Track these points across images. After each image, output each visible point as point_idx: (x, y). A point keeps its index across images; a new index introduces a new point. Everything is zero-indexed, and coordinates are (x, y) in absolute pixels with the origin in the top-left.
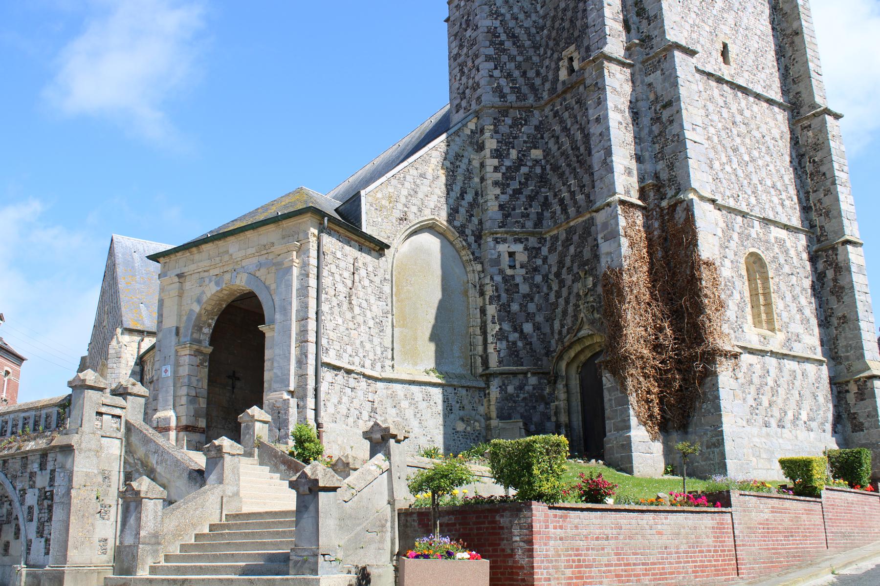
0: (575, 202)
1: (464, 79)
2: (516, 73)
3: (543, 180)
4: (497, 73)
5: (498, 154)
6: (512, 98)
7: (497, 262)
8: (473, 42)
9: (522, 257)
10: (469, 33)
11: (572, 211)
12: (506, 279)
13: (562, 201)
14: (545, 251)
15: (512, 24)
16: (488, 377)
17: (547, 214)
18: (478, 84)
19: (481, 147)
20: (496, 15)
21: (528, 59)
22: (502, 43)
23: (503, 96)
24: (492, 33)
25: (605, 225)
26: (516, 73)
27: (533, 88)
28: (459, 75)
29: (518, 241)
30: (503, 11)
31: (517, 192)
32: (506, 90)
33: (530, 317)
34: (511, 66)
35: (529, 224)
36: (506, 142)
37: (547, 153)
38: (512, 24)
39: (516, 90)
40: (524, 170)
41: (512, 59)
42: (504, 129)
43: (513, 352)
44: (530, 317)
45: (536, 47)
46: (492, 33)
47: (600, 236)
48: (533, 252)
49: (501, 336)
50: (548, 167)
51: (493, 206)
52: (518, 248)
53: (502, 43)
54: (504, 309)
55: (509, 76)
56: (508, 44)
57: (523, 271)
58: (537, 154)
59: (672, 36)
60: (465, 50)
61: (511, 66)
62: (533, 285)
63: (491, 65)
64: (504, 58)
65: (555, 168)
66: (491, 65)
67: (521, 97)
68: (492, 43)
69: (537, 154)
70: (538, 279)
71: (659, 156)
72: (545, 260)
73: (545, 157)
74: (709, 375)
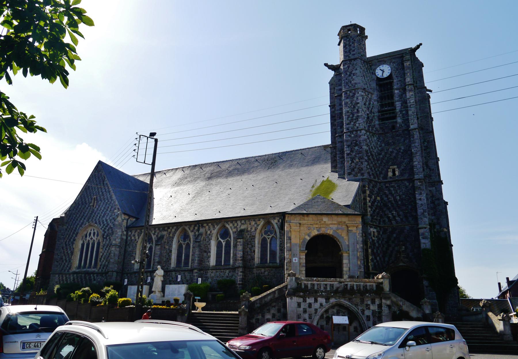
0: (395, 220)
1: (353, 164)
2: (373, 168)
4: (368, 167)
6: (372, 177)
10: (356, 148)
11: (393, 222)
13: (388, 218)
14: (381, 233)
15: (371, 150)
17: (381, 220)
18: (362, 169)
20: (367, 145)
21: (376, 164)
22: (369, 156)
23: (370, 176)
25: (423, 234)
26: (373, 168)
27: (377, 174)
28: (350, 162)
29: (375, 228)
30: (369, 144)
31: (374, 211)
32: (371, 174)
34: (371, 165)
35: (377, 223)
36: (371, 192)
37: (382, 199)
38: (371, 150)
40: (376, 203)
41: (372, 163)
42: (371, 188)
46: (366, 151)
47: (421, 237)
50: (382, 204)
53: (369, 156)
55: (371, 169)
56: (371, 157)
57: (376, 239)
60: (354, 154)
61: (371, 165)
62: (379, 244)
63: (366, 163)
64: (370, 162)
66: (366, 163)
67: (375, 178)
68: (367, 155)
70: (380, 242)
72: (381, 235)
73: (381, 200)
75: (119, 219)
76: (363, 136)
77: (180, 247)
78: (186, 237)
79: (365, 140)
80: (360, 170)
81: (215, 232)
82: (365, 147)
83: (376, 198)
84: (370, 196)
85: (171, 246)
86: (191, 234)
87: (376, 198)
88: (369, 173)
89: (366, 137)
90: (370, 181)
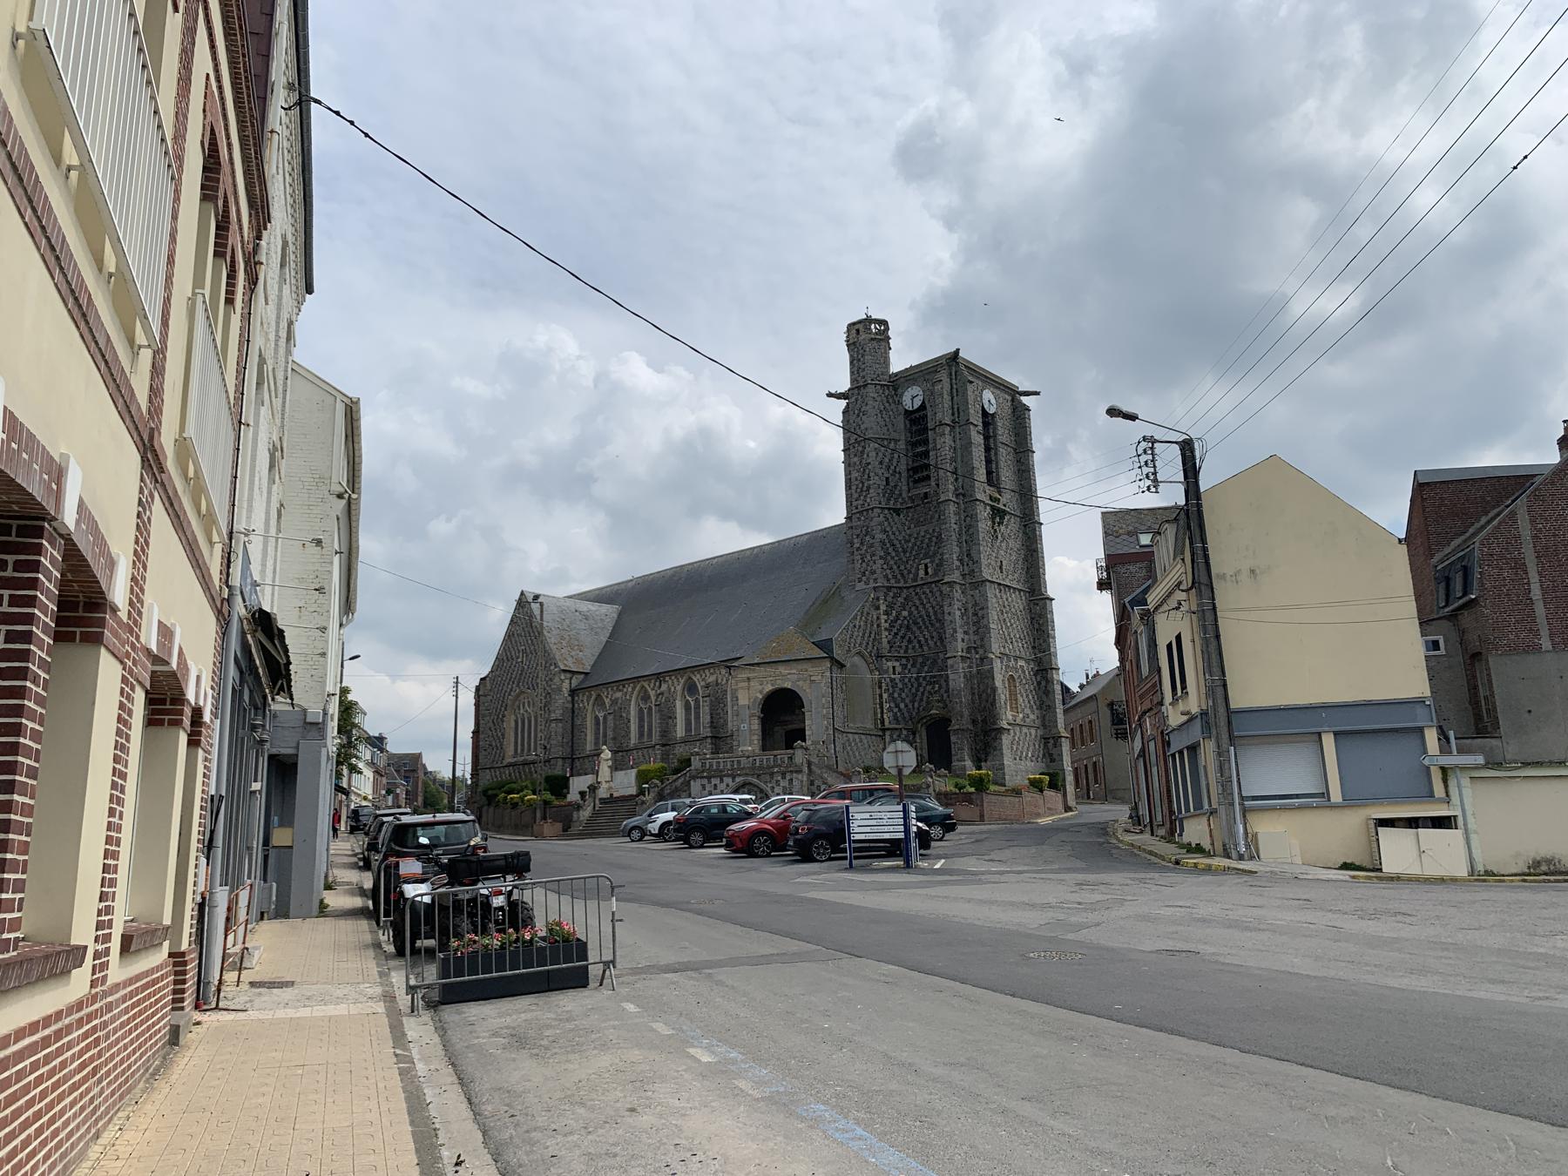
3: (908, 627)
5: (886, 613)
7: (887, 672)
8: (872, 546)
9: (899, 669)
12: (892, 680)
16: (884, 730)
19: (878, 608)
24: (882, 542)
33: (903, 700)
36: (890, 606)
37: (910, 613)
39: (895, 577)
43: (896, 719)
44: (903, 700)
45: (905, 552)
46: (882, 542)
48: (904, 667)
49: (890, 709)
51: (885, 641)
52: (897, 664)
54: (891, 695)
58: (905, 613)
59: (986, 574)
65: (916, 623)
69: (905, 613)
71: (976, 633)
74: (997, 738)
75: (556, 680)
76: (877, 519)
77: (641, 711)
78: (646, 698)
79: (880, 524)
80: (873, 572)
81: (679, 688)
82: (879, 536)
83: (899, 614)
84: (886, 613)
85: (629, 713)
86: (652, 693)
87: (899, 614)
88: (886, 576)
89: (882, 518)
90: (889, 588)
